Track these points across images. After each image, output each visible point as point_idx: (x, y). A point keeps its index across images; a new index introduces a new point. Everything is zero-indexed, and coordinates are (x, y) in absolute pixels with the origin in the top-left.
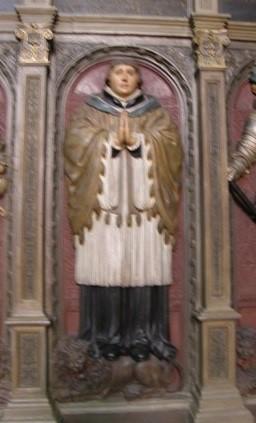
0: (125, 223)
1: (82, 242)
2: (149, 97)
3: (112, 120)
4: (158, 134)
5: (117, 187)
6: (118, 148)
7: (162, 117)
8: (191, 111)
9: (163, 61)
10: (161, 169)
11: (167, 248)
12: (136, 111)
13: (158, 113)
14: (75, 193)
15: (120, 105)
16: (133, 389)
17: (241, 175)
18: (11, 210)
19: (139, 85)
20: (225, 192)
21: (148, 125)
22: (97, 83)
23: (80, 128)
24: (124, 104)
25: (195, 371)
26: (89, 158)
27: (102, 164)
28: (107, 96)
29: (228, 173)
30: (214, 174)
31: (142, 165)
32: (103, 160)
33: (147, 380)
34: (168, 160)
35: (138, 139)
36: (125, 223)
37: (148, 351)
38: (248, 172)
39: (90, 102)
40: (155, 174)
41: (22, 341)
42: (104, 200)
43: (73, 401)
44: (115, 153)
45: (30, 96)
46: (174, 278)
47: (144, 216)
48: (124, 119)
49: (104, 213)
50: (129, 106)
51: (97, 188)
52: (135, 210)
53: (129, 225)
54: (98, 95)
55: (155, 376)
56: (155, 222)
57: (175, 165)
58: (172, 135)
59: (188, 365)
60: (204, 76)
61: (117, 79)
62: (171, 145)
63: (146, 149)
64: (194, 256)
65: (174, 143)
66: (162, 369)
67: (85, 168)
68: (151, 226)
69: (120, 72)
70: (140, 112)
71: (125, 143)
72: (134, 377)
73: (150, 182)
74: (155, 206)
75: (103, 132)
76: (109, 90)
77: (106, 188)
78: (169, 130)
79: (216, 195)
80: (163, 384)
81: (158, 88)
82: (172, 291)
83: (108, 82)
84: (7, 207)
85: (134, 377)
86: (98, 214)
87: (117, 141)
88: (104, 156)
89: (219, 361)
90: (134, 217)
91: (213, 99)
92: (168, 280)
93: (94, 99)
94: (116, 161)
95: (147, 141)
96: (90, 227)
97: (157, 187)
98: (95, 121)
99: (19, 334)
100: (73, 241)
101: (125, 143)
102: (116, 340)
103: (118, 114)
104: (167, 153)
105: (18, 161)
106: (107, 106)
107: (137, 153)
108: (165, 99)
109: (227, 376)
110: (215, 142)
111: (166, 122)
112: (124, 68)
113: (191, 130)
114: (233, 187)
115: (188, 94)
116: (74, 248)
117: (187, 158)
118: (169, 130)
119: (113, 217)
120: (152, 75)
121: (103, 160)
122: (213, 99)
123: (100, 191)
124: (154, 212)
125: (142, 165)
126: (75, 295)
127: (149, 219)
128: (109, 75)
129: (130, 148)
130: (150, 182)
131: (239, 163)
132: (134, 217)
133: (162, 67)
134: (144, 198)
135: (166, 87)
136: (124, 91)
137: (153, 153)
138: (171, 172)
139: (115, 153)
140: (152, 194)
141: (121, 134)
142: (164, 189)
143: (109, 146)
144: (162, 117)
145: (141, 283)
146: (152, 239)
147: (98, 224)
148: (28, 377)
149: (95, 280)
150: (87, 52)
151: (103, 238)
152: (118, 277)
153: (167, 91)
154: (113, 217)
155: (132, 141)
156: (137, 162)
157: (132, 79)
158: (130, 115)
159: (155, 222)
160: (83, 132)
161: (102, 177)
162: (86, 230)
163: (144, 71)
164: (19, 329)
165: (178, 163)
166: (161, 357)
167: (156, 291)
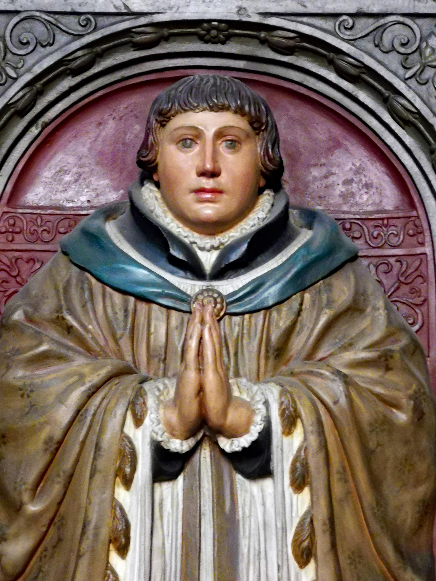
2: (311, 218)
3: (159, 325)
4: (339, 387)
6: (177, 445)
7: (356, 308)
9: (361, 75)
10: (348, 522)
12: (257, 286)
13: (342, 290)
15: (192, 268)
19: (270, 177)
21: (299, 343)
22: (109, 161)
23: (43, 359)
24: (208, 260)
27: (116, 507)
28: (151, 236)
31: (272, 507)
32: (122, 495)
34: (375, 483)
35: (258, 403)
39: (80, 242)
40: (322, 543)
44: (167, 465)
48: (203, 333)
50: (222, 271)
54: (109, 212)
58: (397, 385)
61: (181, 163)
62: (386, 424)
63: (287, 448)
65: (402, 417)
67: (55, 518)
69: (189, 139)
70: (270, 293)
71: (204, 428)
76: (150, 198)
78: (383, 362)
81: (349, 182)
83: (149, 170)
87: (174, 417)
88: (128, 482)
93: (96, 239)
94: (172, 492)
95: (290, 421)
98: (94, 330)
101: (204, 428)
103: (181, 304)
104: (368, 456)
106: (144, 269)
107: (255, 461)
108: (383, 221)
111: (374, 324)
112: (208, 121)
118: (383, 362)
120: (323, 129)
121: (122, 495)
125: (272, 507)
128: (147, 146)
129: (226, 444)
133: (363, 96)
135: (376, 173)
136: (208, 211)
137: (315, 463)
138: (391, 529)
141: (190, 388)
143: (142, 440)
144: (356, 308)
150: (65, 46)
153: (388, 197)
155: (233, 417)
157: (236, 165)
160: (51, 377)
161: (114, 559)
163: (288, 118)
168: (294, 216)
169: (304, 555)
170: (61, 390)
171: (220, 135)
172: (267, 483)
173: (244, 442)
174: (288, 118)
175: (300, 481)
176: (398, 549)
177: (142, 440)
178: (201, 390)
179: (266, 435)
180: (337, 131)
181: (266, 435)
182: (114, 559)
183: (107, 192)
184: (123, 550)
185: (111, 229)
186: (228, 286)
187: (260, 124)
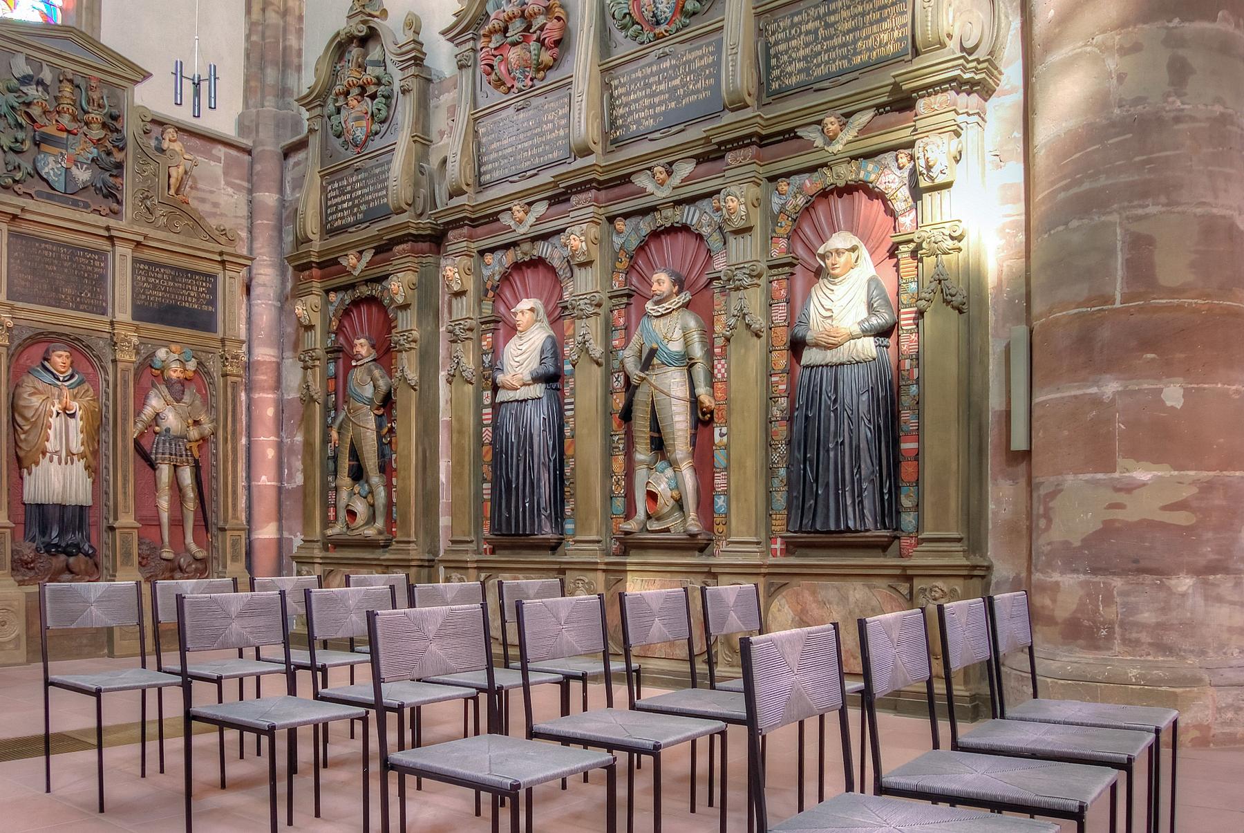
1: (30, 474)
9: (87, 346)
11: (90, 481)
17: (142, 434)
20: (131, 445)
25: (110, 565)
29: (133, 432)
30: (124, 433)
35: (75, 406)
42: (50, 446)
47: (75, 458)
52: (70, 453)
56: (82, 462)
57: (96, 425)
58: (96, 404)
59: (105, 563)
60: (120, 365)
63: (79, 413)
68: (80, 465)
69: (60, 356)
73: (81, 436)
74: (84, 452)
79: (125, 447)
80: (87, 573)
86: (44, 453)
89: (127, 555)
91: (125, 382)
92: (90, 503)
96: (37, 464)
103: (57, 386)
107: (73, 416)
114: (136, 442)
116: (21, 478)
119: (56, 458)
124: (82, 456)
130: (81, 436)
131: (140, 425)
134: (76, 445)
139: (58, 414)
140: (82, 444)
143: (54, 410)
147: (44, 462)
154: (56, 458)
156: (72, 422)
158: (70, 387)
159: (82, 462)
166: (86, 554)
170: (36, 401)
177: (54, 410)
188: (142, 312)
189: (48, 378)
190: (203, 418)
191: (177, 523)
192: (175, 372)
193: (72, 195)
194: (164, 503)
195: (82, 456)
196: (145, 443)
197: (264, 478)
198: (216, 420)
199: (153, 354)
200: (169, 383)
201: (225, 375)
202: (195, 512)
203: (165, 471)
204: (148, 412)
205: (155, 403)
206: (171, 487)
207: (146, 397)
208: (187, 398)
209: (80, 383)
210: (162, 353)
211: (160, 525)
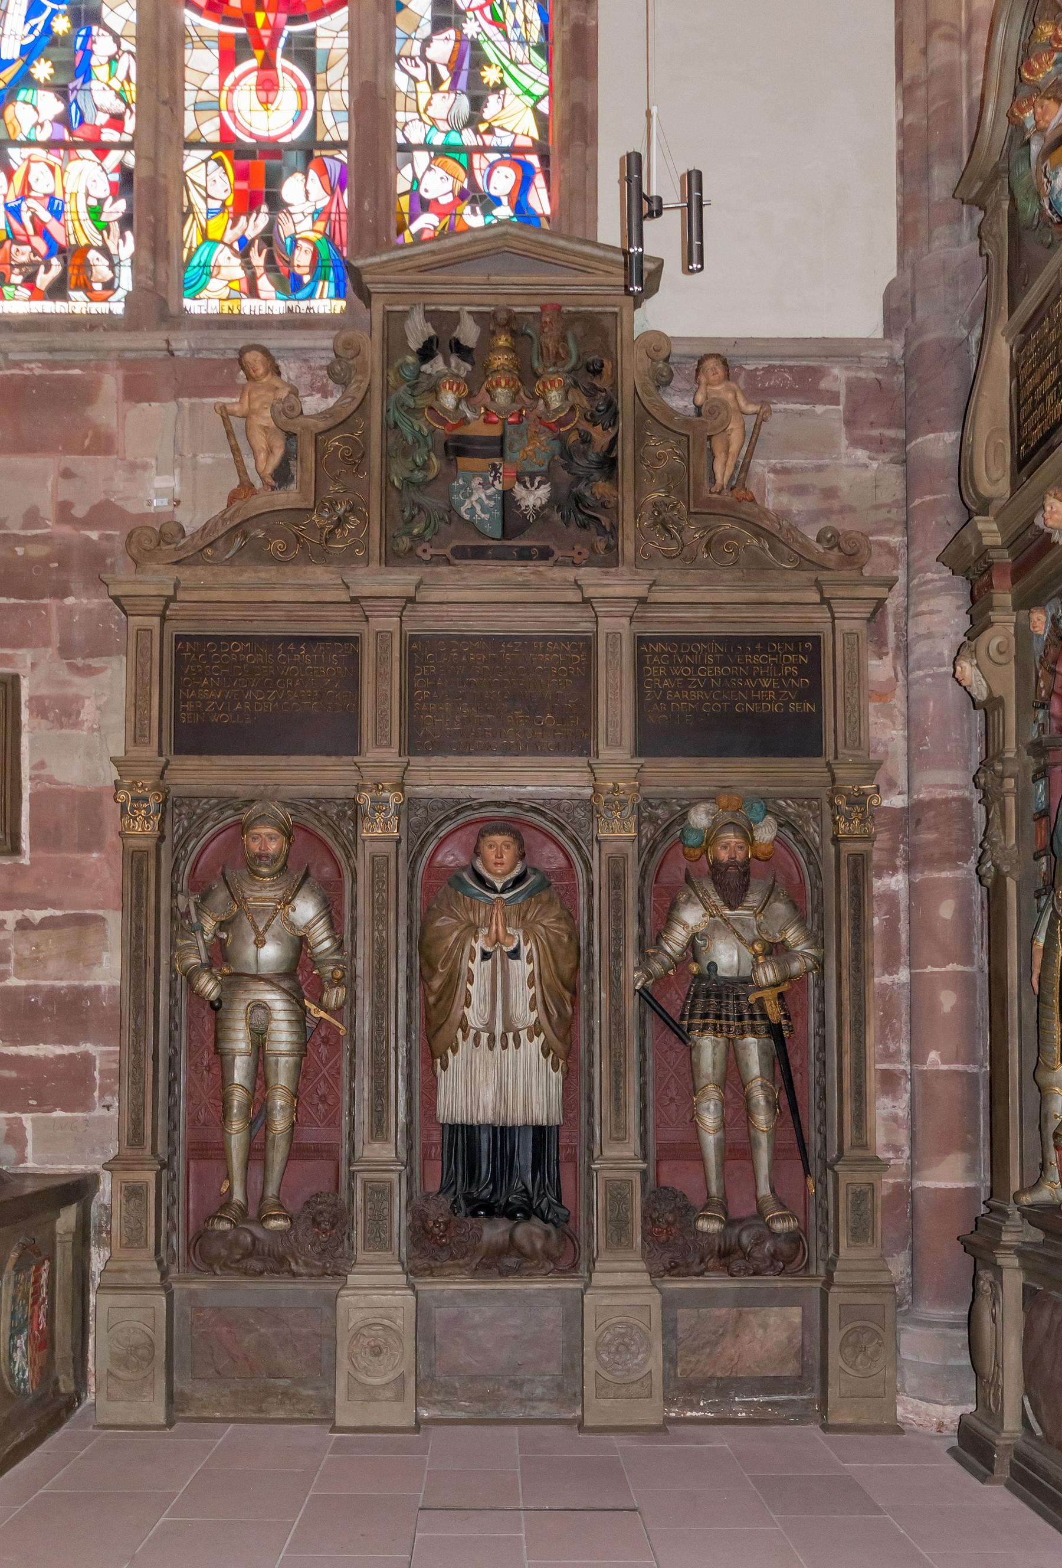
0: (498, 1044)
1: (445, 1067)
2: (535, 871)
5: (488, 998)
6: (489, 949)
8: (591, 895)
14: (435, 1005)
15: (494, 890)
16: (511, 1262)
18: (352, 1027)
20: (631, 1005)
26: (454, 965)
28: (480, 879)
29: (634, 978)
31: (521, 969)
33: (527, 1248)
34: (555, 961)
36: (498, 1044)
37: (528, 1211)
38: (671, 972)
41: (369, 1191)
43: (431, 1275)
44: (485, 956)
45: (376, 880)
46: (565, 1115)
47: (523, 1034)
49: (472, 1032)
50: (503, 891)
51: (463, 1001)
53: (505, 1046)
55: (539, 1244)
56: (539, 1040)
57: (566, 968)
61: (491, 854)
63: (524, 951)
64: (591, 1088)
66: (548, 1234)
72: (511, 1246)
75: (473, 929)
77: (474, 1000)
82: (563, 1133)
84: (347, 1022)
85: (511, 1246)
90: (510, 1035)
91: (617, 880)
92: (556, 1119)
93: (460, 879)
96: (455, 1051)
97: (539, 998)
99: (365, 1183)
100: (433, 1065)
102: (486, 1194)
105: (362, 965)
107: (515, 954)
109: (630, 1246)
110: (618, 937)
113: (590, 919)
114: (645, 996)
115: (589, 869)
117: (584, 958)
119: (484, 1036)
120: (541, 838)
122: (617, 880)
123: (468, 1004)
125: (521, 969)
126: (436, 1138)
127: (531, 1040)
128: (477, 847)
132: (510, 1035)
138: (559, 976)
142: (549, 1000)
145: (520, 1123)
146: (534, 1066)
147: (465, 1046)
148: (377, 1239)
149: (461, 1117)
151: (470, 1062)
152: (490, 1112)
154: (484, 1036)
159: (539, 1040)
162: (449, 1051)
164: (366, 1175)
165: (572, 965)
167: (541, 1134)
168: (529, 871)
169: (531, 985)
171: (503, 843)
172: (519, 961)
173: (511, 948)
174: (527, 834)
175: (530, 960)
176: (563, 984)
178: (497, 932)
179: (519, 945)
180: (545, 839)
181: (519, 945)
182: (469, 986)
183: (463, 860)
184: (471, 984)
185: (465, 876)
186: (505, 896)
187: (518, 837)
188: (649, 741)
189: (477, 888)
190: (792, 935)
191: (737, 1150)
192: (729, 847)
193: (514, 536)
194: (710, 1119)
195: (535, 1030)
196: (674, 1002)
197: (933, 1055)
198: (817, 940)
199: (684, 817)
200: (717, 871)
201: (836, 840)
202: (774, 1134)
203: (708, 1049)
204: (679, 936)
205: (692, 916)
206: (723, 1084)
207: (674, 906)
208: (753, 899)
209: (530, 893)
210: (700, 818)
211: (702, 1159)
